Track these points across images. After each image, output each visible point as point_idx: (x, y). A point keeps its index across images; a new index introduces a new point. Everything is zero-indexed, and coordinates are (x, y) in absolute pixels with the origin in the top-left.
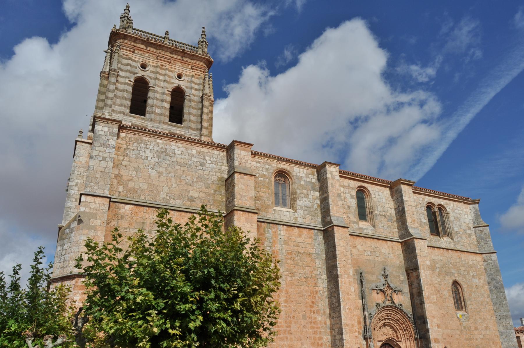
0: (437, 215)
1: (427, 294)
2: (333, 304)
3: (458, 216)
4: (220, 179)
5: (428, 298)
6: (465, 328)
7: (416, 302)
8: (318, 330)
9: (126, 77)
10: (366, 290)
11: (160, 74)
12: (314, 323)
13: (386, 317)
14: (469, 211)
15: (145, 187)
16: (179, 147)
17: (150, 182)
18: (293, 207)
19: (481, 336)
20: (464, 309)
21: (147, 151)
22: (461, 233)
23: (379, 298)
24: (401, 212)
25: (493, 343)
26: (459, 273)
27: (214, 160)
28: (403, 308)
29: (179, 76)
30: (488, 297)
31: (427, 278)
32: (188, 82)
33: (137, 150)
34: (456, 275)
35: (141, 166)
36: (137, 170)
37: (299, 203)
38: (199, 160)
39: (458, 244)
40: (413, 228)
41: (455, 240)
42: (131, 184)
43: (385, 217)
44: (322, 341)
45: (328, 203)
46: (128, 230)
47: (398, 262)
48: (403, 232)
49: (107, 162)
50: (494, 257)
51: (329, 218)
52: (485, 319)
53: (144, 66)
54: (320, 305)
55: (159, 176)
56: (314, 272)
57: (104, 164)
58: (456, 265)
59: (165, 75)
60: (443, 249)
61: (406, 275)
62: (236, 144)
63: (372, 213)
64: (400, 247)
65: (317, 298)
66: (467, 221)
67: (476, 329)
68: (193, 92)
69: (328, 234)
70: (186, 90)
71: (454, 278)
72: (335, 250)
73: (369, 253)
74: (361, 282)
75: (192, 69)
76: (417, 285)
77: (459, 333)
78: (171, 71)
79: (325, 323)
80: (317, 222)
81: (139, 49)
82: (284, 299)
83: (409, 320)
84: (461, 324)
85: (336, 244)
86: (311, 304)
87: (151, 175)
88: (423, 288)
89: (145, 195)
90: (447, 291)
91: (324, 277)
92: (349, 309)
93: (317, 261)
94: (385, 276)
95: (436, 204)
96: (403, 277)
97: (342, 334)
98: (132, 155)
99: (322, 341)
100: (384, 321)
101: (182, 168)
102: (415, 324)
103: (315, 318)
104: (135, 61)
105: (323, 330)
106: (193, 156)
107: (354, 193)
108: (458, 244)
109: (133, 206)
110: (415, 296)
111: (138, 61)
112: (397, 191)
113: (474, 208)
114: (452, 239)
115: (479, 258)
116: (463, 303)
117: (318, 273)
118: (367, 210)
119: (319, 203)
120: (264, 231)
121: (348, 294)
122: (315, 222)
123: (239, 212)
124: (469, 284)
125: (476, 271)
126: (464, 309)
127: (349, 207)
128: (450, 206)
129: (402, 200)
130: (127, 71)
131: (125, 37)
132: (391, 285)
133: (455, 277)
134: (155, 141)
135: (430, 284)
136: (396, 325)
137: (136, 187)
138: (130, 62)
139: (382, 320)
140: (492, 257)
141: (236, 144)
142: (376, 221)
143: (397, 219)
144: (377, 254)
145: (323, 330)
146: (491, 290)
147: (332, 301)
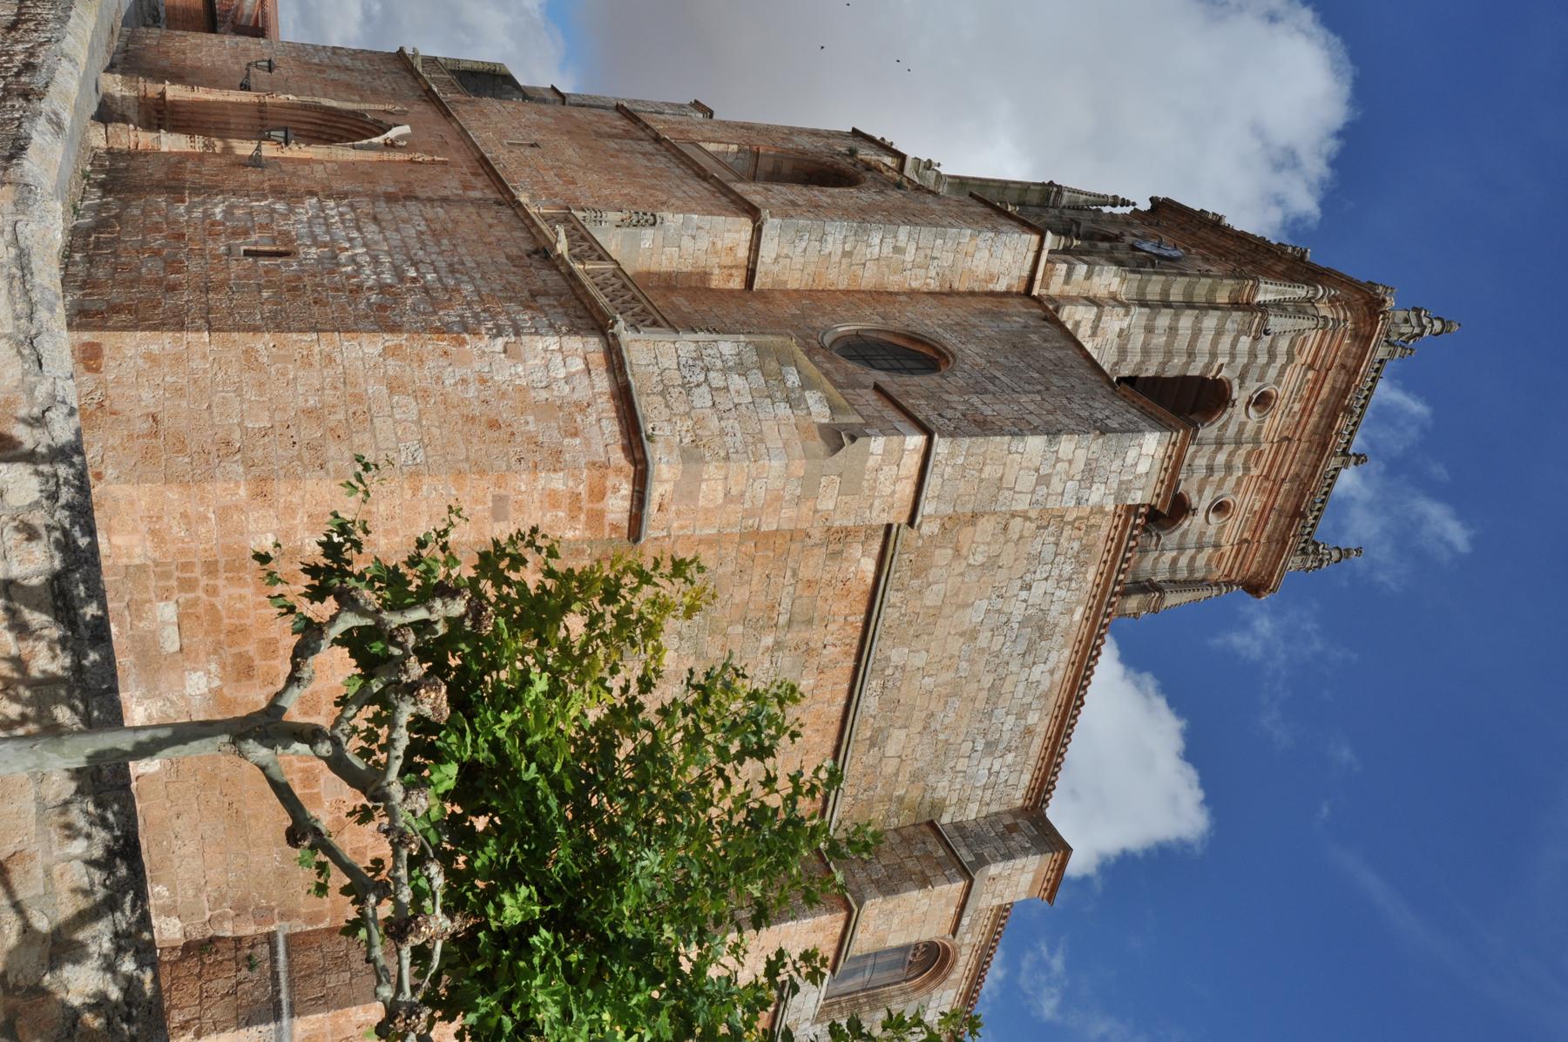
4: (938, 807)
9: (1233, 356)
11: (1231, 454)
15: (931, 598)
16: (1052, 672)
17: (947, 611)
21: (1049, 586)
27: (1003, 777)
29: (1221, 508)
32: (1202, 534)
33: (1056, 555)
35: (1001, 575)
36: (992, 564)
38: (1006, 736)
42: (943, 555)
46: (789, 578)
49: (1033, 492)
53: (1263, 401)
55: (962, 634)
57: (1027, 481)
59: (1229, 468)
62: (1058, 856)
68: (1169, 556)
70: (1177, 534)
75: (1242, 541)
78: (1239, 482)
81: (1318, 383)
87: (969, 610)
89: (905, 602)
98: (1042, 544)
101: (983, 695)
104: (1281, 373)
106: (1020, 716)
109: (870, 581)
111: (1278, 382)
123: (841, 924)
130: (1253, 355)
131: (1363, 339)
134: (1078, 603)
137: (933, 574)
138: (1281, 360)
141: (1058, 856)
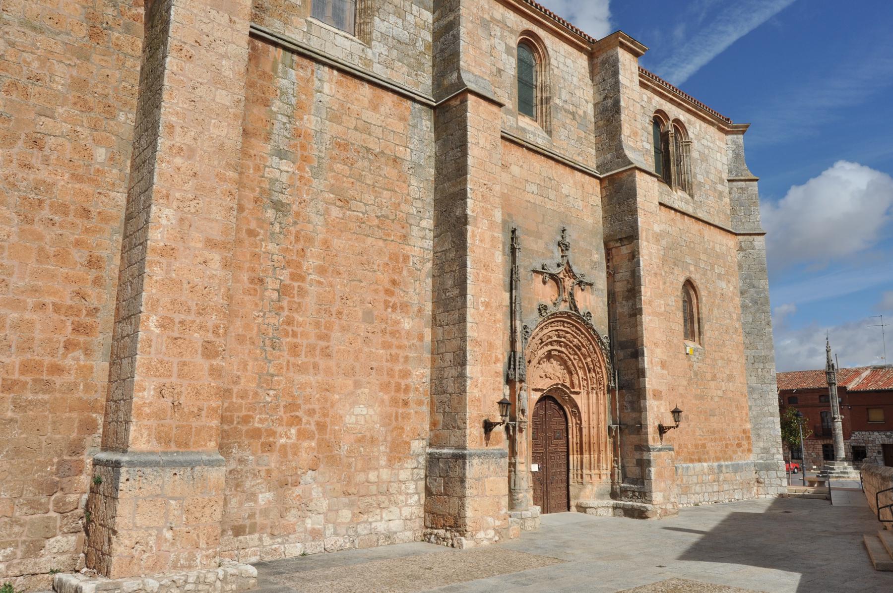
0: (671, 139)
1: (649, 294)
2: (445, 291)
3: (706, 152)
5: (650, 302)
6: (696, 374)
7: (619, 310)
8: (402, 354)
10: (522, 272)
12: (393, 334)
13: (555, 338)
14: (725, 146)
18: (362, 32)
19: (720, 393)
20: (697, 338)
22: (707, 187)
23: (545, 293)
24: (609, 114)
25: (737, 407)
26: (697, 266)
28: (593, 321)
30: (738, 320)
31: (651, 259)
34: (692, 268)
37: (379, 25)
39: (700, 207)
40: (632, 148)
41: (696, 198)
43: (574, 119)
44: (409, 381)
45: (456, 37)
47: (590, 221)
48: (609, 156)
50: (759, 242)
51: (455, 75)
52: (729, 361)
54: (411, 290)
56: (404, 207)
58: (693, 249)
60: (676, 210)
61: (603, 251)
63: (547, 100)
64: (598, 189)
65: (405, 273)
66: (719, 166)
67: (714, 378)
69: (448, 110)
71: (688, 274)
72: (465, 154)
73: (534, 188)
74: (513, 250)
76: (629, 274)
77: (685, 383)
79: (421, 338)
80: (422, 84)
82: (318, 262)
83: (601, 349)
84: (691, 366)
85: (470, 139)
86: (388, 286)
88: (642, 280)
90: (673, 298)
91: (428, 223)
92: (487, 305)
93: (414, 182)
94: (564, 246)
95: (672, 118)
96: (599, 256)
97: (463, 363)
99: (409, 381)
100: (550, 347)
102: (612, 357)
103: (397, 323)
105: (412, 354)
107: (514, 41)
108: (700, 207)
110: (620, 299)
112: (604, 63)
113: (734, 142)
114: (692, 196)
115: (731, 242)
116: (696, 325)
117: (413, 211)
118: (537, 94)
119: (430, 39)
120: (274, 69)
121: (486, 267)
122: (417, 84)
124: (711, 289)
125: (724, 267)
126: (697, 338)
127: (499, 71)
128: (696, 128)
129: (617, 83)
132: (575, 269)
133: (690, 272)
135: (656, 274)
136: (572, 357)
139: (547, 345)
140: (755, 243)
142: (555, 122)
143: (597, 127)
144: (552, 194)
145: (412, 354)
146: (744, 307)
147: (442, 283)
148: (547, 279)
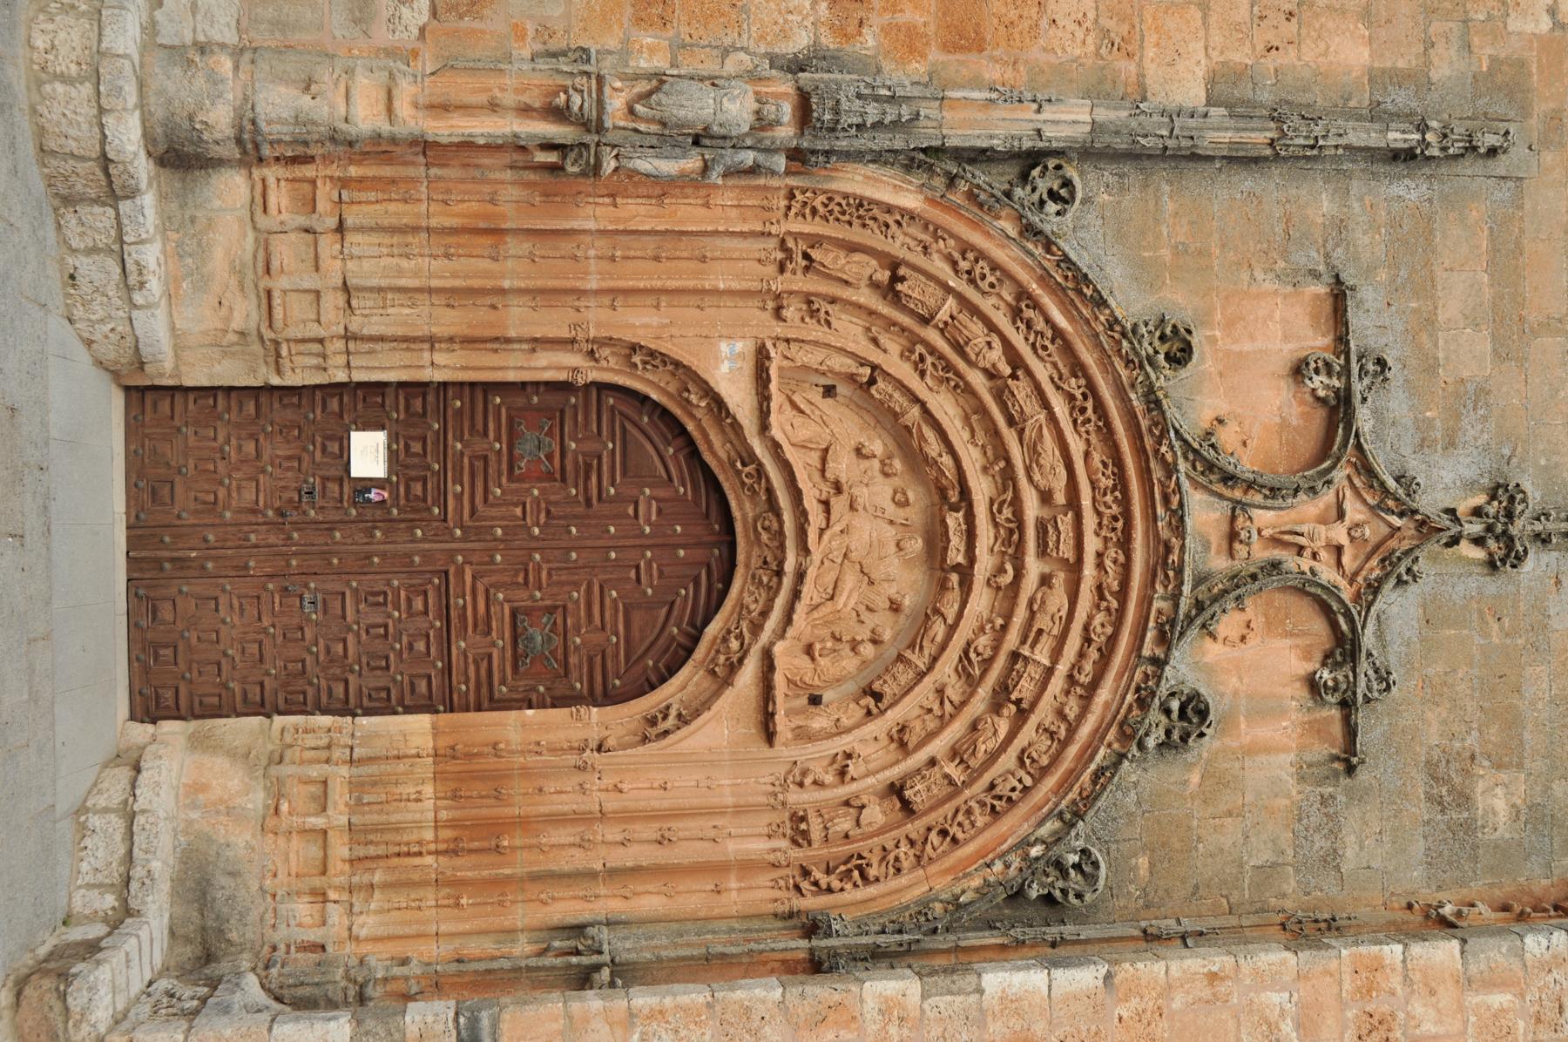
13: (1032, 508)
100: (982, 489)
148: (1319, 383)
